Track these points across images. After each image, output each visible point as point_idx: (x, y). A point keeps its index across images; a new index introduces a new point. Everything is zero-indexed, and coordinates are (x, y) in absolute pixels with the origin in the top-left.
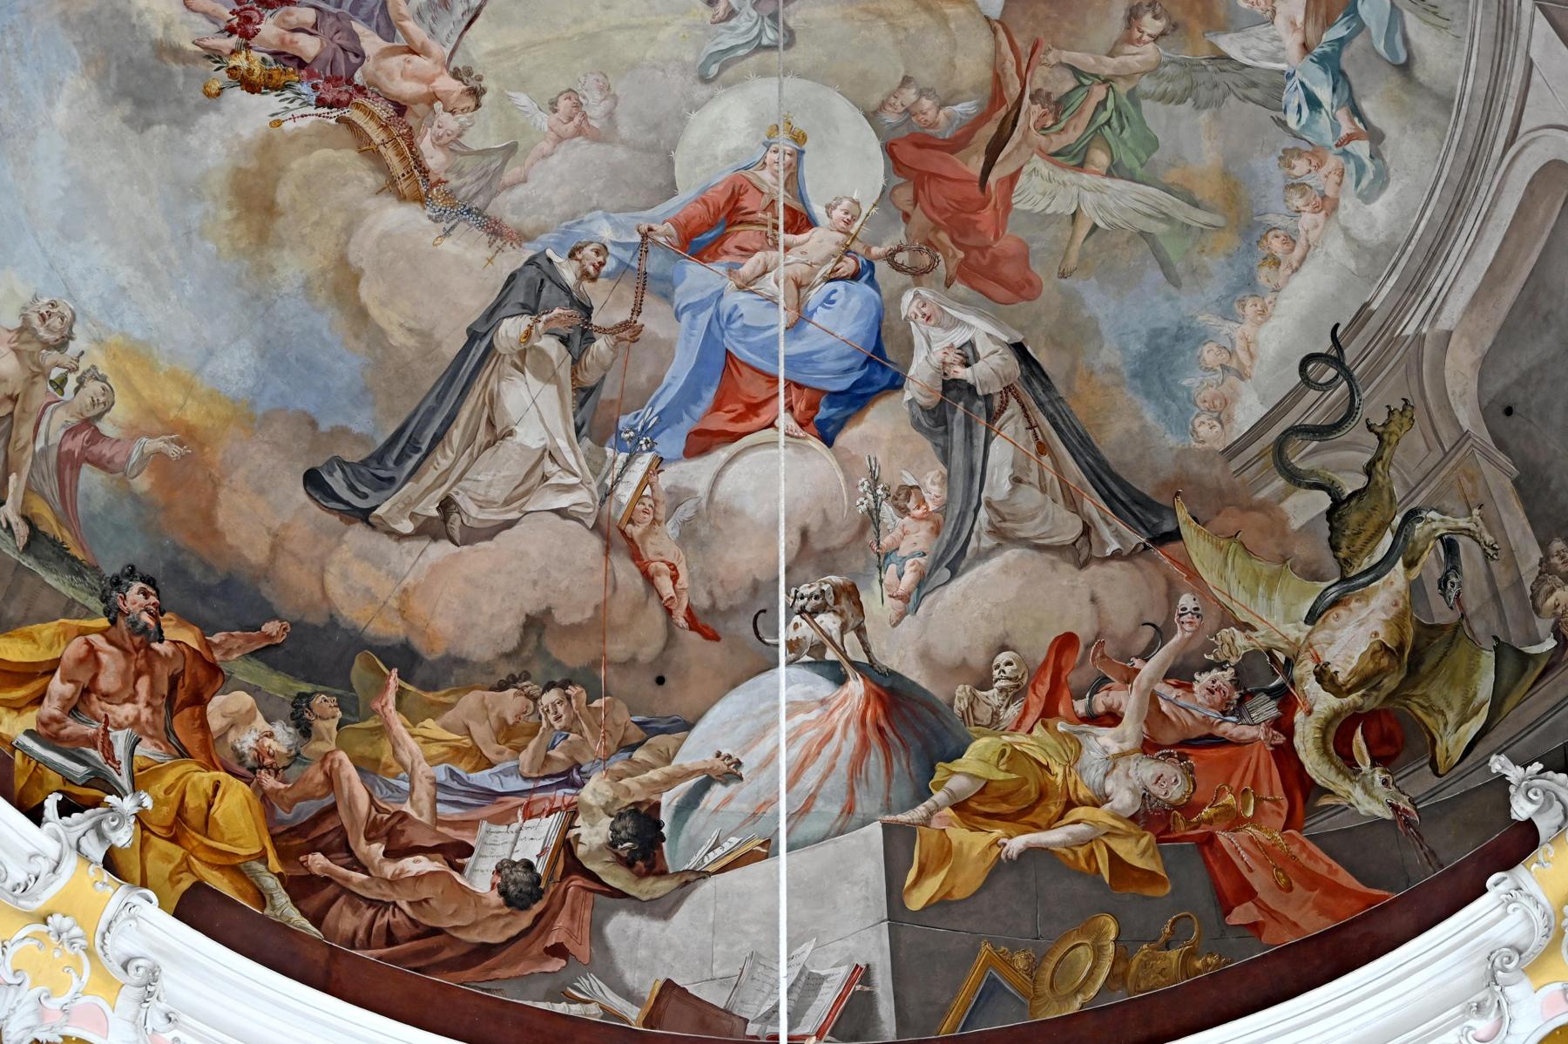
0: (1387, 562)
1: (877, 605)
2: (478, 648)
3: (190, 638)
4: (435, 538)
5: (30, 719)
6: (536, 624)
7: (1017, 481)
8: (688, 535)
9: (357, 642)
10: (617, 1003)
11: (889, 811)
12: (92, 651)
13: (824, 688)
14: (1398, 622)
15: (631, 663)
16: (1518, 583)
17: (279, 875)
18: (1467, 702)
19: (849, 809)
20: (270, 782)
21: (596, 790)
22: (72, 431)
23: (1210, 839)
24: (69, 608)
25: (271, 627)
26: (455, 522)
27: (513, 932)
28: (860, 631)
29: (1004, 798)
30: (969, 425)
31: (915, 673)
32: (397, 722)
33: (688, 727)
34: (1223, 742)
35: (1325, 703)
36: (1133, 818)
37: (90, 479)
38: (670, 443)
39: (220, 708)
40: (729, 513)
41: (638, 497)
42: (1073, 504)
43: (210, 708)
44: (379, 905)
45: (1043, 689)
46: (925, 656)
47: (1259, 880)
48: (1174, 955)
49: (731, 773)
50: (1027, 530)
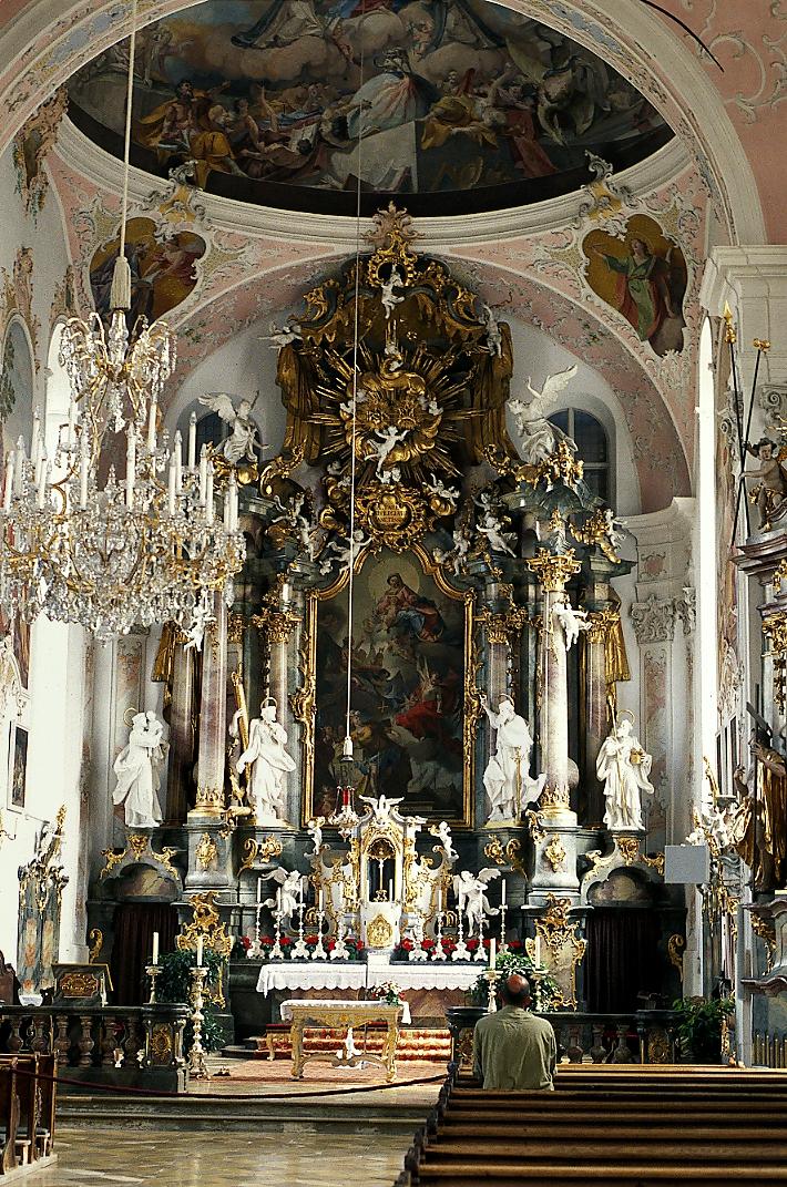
0: (564, 70)
1: (413, 56)
2: (289, 77)
3: (201, 94)
4: (273, 47)
5: (160, 138)
6: (306, 67)
7: (455, 25)
8: (352, 38)
9: (251, 81)
10: (335, 182)
11: (416, 117)
12: (174, 108)
13: (397, 80)
14: (568, 86)
15: (337, 75)
16: (602, 86)
17: (235, 161)
18: (586, 116)
19: (405, 117)
20: (229, 130)
21: (327, 114)
22: (161, 49)
23: (511, 138)
24: (166, 98)
25: (225, 84)
26: (279, 41)
27: (304, 163)
28: (408, 63)
29: (451, 115)
30: (441, 10)
31: (425, 76)
32: (264, 101)
33: (355, 93)
34: (519, 109)
35: (547, 104)
36: (490, 128)
37: (168, 60)
38: (346, 14)
39: (212, 112)
40: (365, 31)
41: (336, 28)
42: (474, 33)
43: (210, 113)
44: (264, 162)
45: (464, 84)
46: (428, 71)
47: (524, 154)
48: (499, 173)
49: (368, 106)
50: (459, 38)
